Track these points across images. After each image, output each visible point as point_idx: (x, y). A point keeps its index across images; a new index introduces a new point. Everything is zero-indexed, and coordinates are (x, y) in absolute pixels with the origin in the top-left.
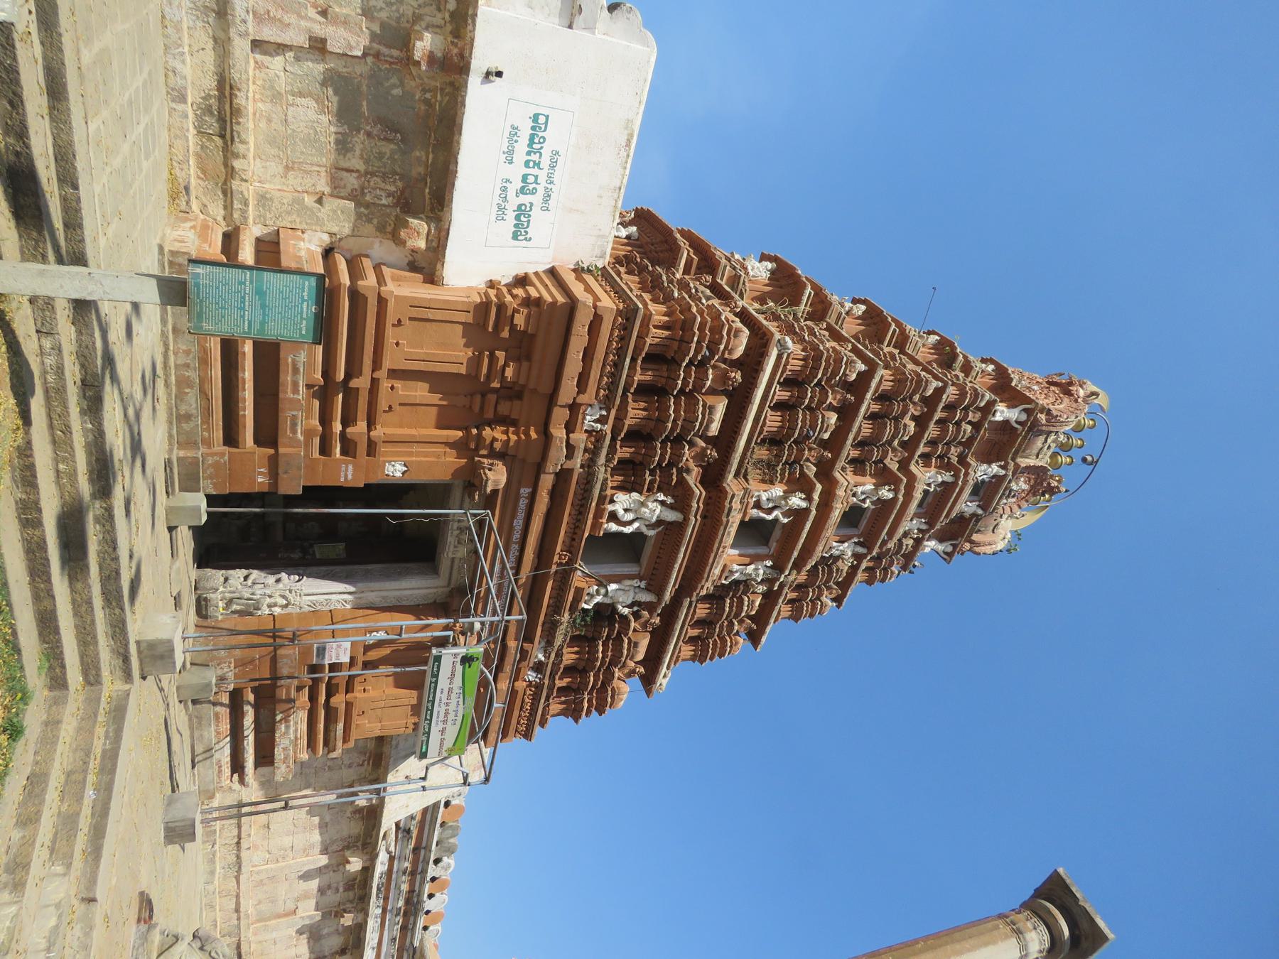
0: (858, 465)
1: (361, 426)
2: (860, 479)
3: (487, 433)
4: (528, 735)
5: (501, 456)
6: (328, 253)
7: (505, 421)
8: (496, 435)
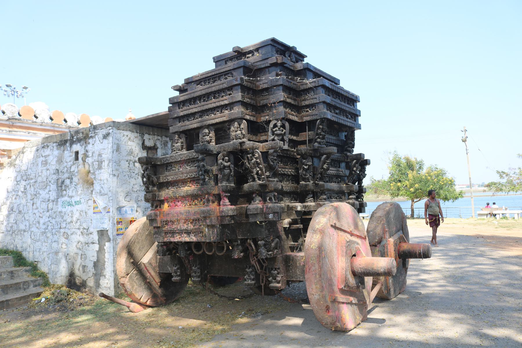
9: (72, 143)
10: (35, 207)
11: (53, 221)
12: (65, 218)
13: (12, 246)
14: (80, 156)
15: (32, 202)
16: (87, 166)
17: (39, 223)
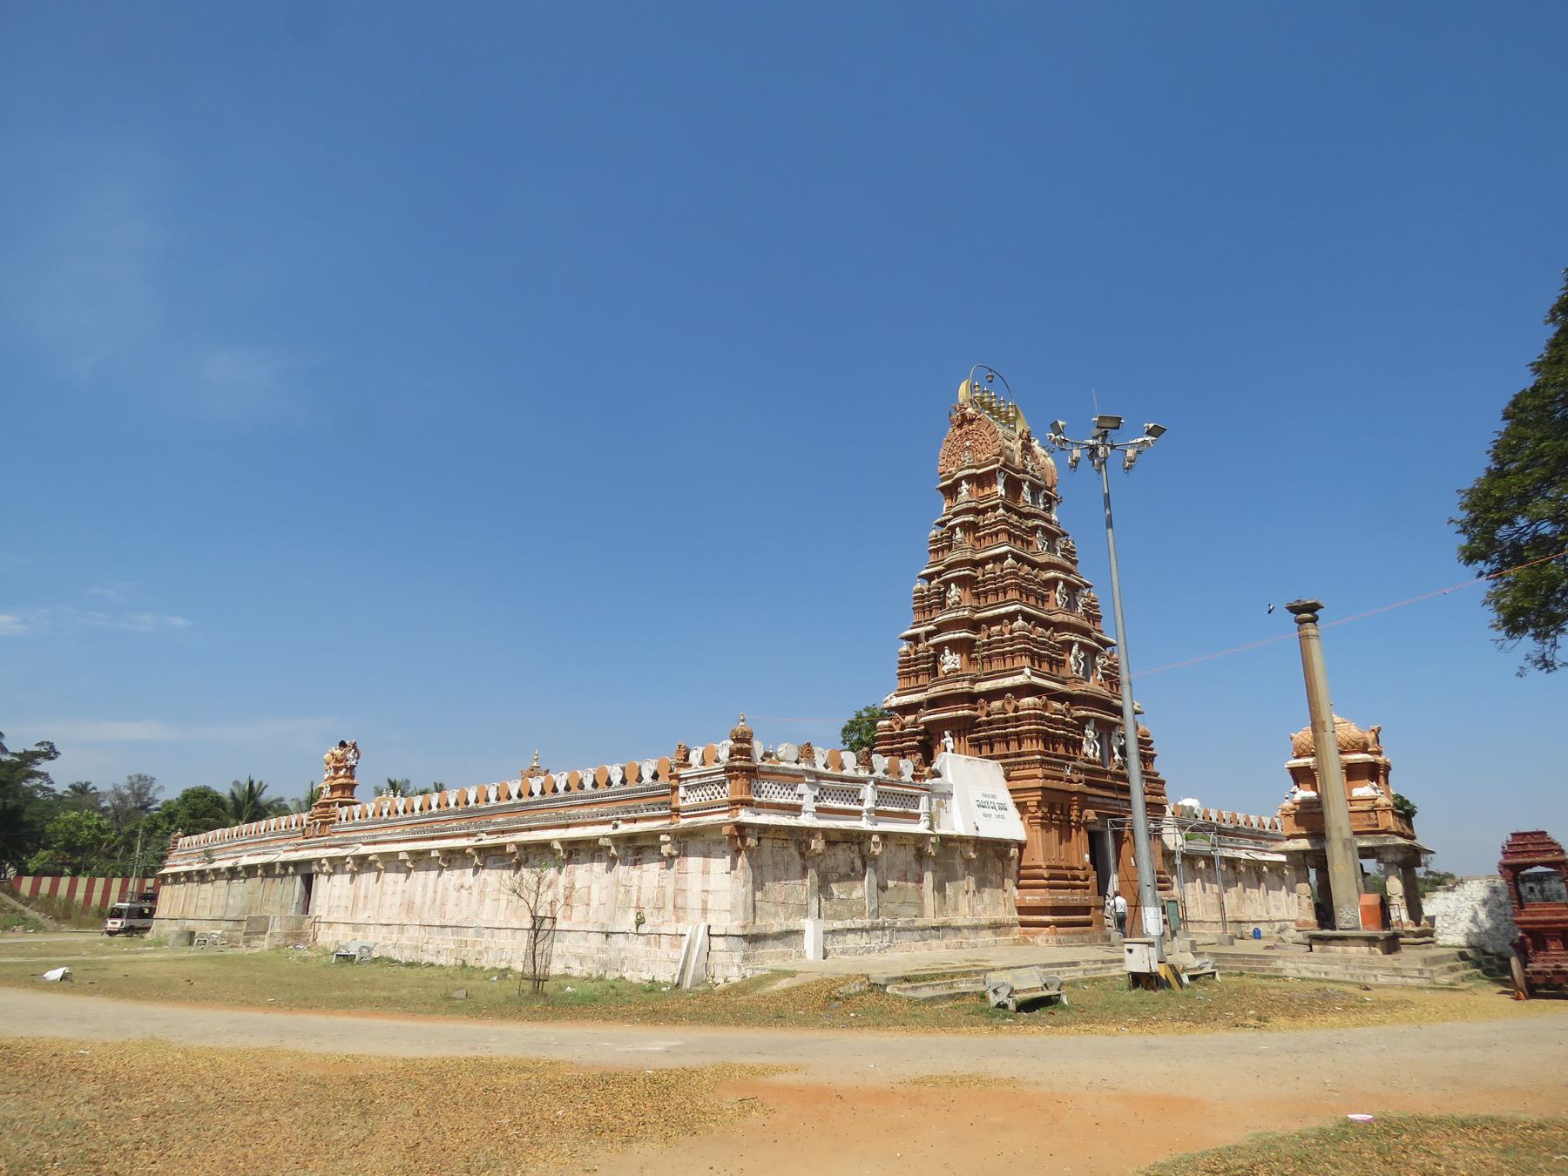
0: (1044, 599)
1: (1076, 872)
2: (1051, 599)
3: (1074, 818)
4: (1163, 783)
5: (1081, 811)
6: (1019, 887)
7: (1069, 809)
8: (1074, 813)
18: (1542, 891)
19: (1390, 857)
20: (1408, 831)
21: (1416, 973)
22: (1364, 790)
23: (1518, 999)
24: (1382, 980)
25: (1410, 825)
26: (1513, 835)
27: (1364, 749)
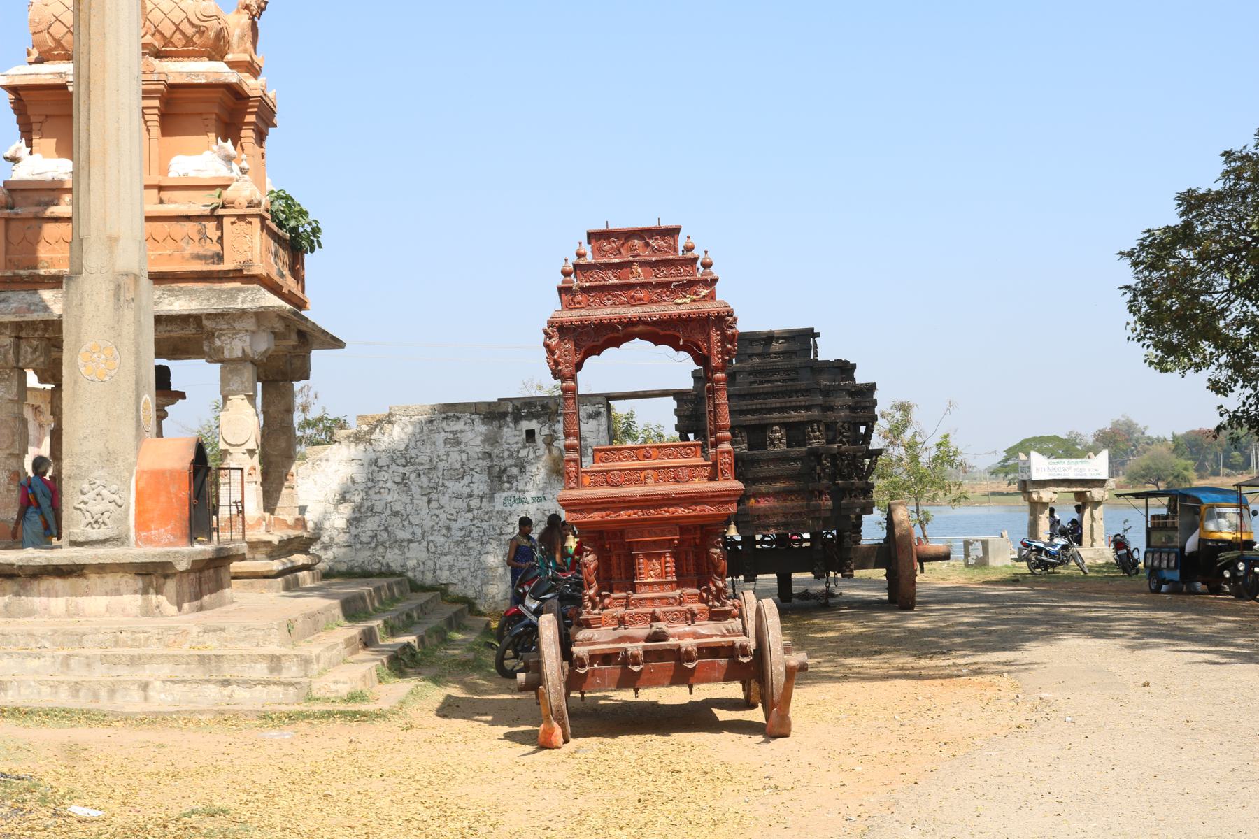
9: (518, 418)
10: (434, 504)
11: (485, 525)
12: (510, 520)
13: (376, 566)
14: (539, 439)
15: (425, 499)
16: (555, 452)
17: (448, 528)
18: (550, 441)
19: (236, 346)
20: (290, 284)
21: (260, 671)
22: (201, 159)
23: (545, 745)
24: (163, 698)
25: (297, 274)
26: (593, 236)
27: (217, 49)
